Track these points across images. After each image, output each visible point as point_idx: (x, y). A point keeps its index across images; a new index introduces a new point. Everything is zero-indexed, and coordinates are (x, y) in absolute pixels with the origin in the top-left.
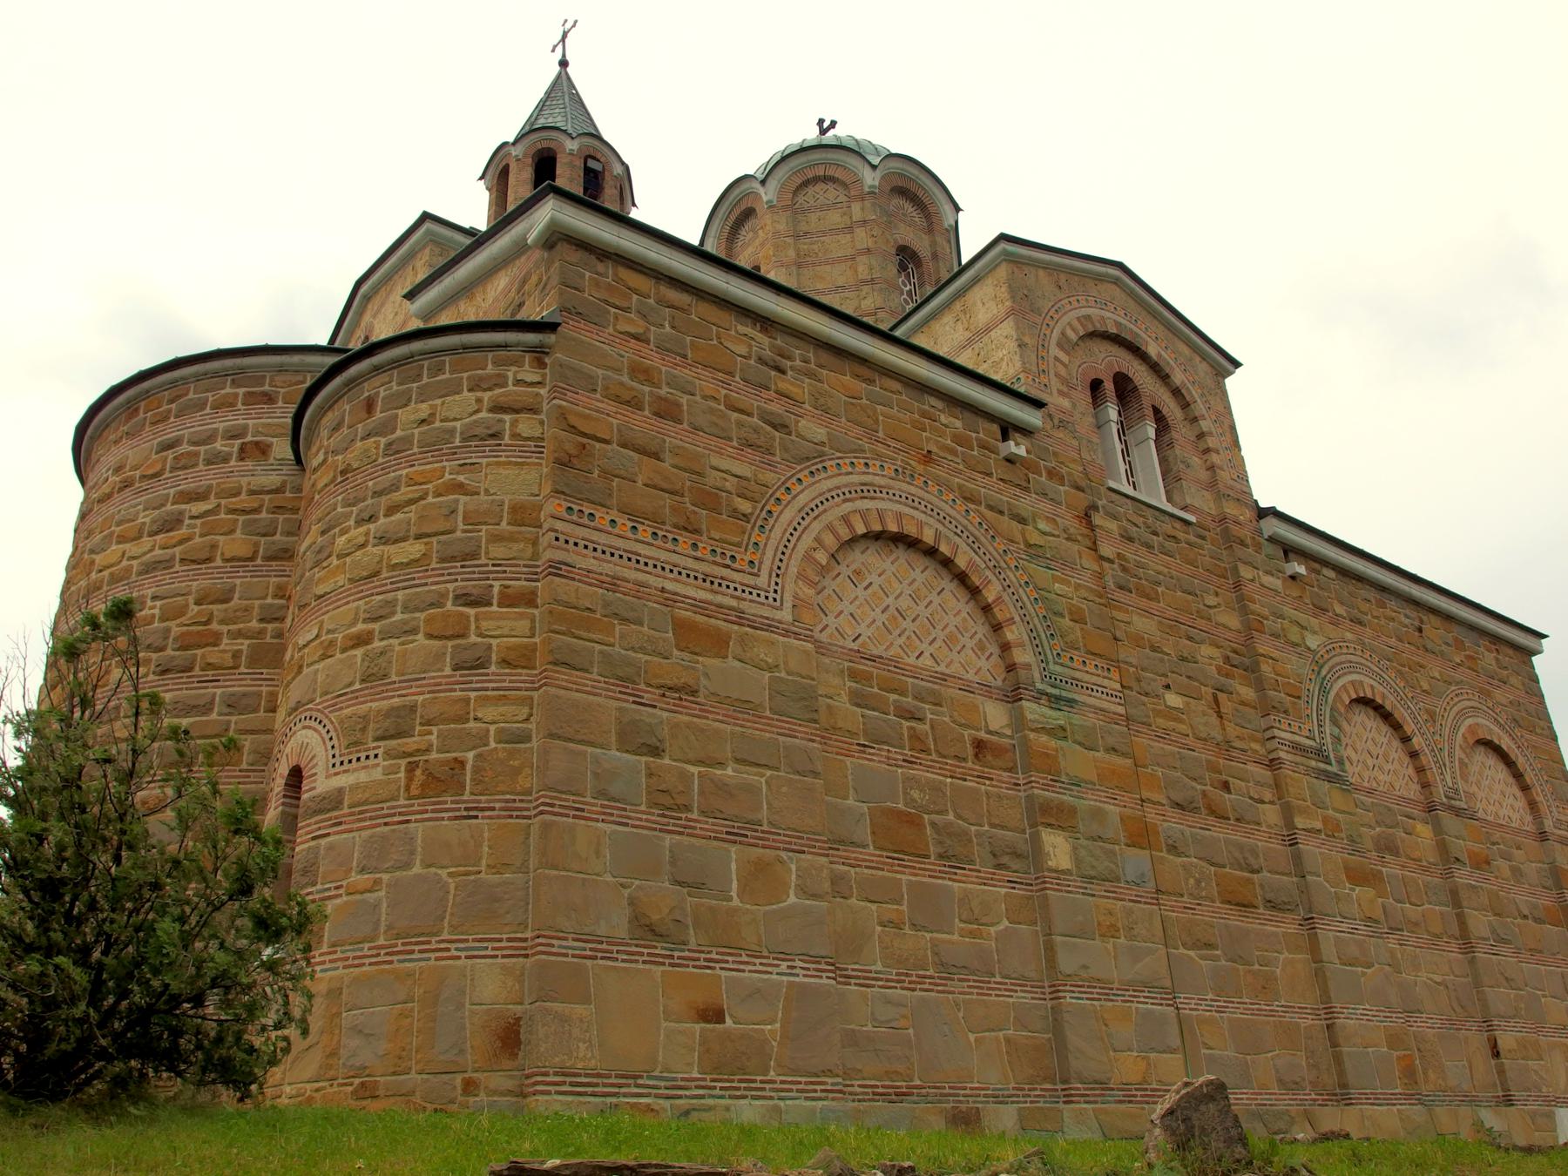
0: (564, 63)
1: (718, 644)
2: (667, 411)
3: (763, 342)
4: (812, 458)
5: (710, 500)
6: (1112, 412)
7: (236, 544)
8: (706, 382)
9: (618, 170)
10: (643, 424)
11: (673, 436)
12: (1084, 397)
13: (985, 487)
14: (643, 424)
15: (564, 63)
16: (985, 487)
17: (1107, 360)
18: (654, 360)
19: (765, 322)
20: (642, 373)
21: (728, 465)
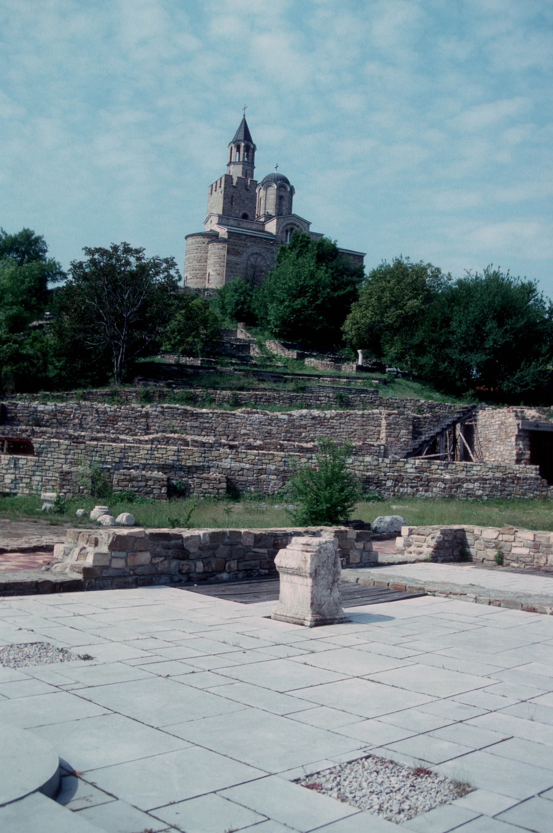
0: (244, 115)
1: (238, 264)
2: (236, 245)
3: (245, 236)
4: (248, 247)
5: (239, 253)
6: (289, 233)
7: (202, 252)
8: (239, 242)
9: (252, 147)
10: (234, 247)
11: (236, 247)
12: (284, 234)
13: (267, 247)
14: (234, 247)
15: (244, 115)
16: (267, 247)
17: (289, 227)
18: (235, 241)
19: (246, 235)
20: (234, 242)
21: (240, 249)
